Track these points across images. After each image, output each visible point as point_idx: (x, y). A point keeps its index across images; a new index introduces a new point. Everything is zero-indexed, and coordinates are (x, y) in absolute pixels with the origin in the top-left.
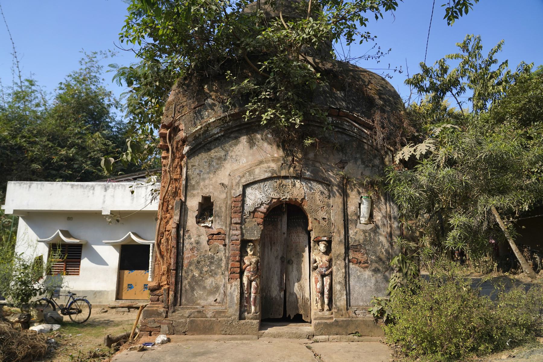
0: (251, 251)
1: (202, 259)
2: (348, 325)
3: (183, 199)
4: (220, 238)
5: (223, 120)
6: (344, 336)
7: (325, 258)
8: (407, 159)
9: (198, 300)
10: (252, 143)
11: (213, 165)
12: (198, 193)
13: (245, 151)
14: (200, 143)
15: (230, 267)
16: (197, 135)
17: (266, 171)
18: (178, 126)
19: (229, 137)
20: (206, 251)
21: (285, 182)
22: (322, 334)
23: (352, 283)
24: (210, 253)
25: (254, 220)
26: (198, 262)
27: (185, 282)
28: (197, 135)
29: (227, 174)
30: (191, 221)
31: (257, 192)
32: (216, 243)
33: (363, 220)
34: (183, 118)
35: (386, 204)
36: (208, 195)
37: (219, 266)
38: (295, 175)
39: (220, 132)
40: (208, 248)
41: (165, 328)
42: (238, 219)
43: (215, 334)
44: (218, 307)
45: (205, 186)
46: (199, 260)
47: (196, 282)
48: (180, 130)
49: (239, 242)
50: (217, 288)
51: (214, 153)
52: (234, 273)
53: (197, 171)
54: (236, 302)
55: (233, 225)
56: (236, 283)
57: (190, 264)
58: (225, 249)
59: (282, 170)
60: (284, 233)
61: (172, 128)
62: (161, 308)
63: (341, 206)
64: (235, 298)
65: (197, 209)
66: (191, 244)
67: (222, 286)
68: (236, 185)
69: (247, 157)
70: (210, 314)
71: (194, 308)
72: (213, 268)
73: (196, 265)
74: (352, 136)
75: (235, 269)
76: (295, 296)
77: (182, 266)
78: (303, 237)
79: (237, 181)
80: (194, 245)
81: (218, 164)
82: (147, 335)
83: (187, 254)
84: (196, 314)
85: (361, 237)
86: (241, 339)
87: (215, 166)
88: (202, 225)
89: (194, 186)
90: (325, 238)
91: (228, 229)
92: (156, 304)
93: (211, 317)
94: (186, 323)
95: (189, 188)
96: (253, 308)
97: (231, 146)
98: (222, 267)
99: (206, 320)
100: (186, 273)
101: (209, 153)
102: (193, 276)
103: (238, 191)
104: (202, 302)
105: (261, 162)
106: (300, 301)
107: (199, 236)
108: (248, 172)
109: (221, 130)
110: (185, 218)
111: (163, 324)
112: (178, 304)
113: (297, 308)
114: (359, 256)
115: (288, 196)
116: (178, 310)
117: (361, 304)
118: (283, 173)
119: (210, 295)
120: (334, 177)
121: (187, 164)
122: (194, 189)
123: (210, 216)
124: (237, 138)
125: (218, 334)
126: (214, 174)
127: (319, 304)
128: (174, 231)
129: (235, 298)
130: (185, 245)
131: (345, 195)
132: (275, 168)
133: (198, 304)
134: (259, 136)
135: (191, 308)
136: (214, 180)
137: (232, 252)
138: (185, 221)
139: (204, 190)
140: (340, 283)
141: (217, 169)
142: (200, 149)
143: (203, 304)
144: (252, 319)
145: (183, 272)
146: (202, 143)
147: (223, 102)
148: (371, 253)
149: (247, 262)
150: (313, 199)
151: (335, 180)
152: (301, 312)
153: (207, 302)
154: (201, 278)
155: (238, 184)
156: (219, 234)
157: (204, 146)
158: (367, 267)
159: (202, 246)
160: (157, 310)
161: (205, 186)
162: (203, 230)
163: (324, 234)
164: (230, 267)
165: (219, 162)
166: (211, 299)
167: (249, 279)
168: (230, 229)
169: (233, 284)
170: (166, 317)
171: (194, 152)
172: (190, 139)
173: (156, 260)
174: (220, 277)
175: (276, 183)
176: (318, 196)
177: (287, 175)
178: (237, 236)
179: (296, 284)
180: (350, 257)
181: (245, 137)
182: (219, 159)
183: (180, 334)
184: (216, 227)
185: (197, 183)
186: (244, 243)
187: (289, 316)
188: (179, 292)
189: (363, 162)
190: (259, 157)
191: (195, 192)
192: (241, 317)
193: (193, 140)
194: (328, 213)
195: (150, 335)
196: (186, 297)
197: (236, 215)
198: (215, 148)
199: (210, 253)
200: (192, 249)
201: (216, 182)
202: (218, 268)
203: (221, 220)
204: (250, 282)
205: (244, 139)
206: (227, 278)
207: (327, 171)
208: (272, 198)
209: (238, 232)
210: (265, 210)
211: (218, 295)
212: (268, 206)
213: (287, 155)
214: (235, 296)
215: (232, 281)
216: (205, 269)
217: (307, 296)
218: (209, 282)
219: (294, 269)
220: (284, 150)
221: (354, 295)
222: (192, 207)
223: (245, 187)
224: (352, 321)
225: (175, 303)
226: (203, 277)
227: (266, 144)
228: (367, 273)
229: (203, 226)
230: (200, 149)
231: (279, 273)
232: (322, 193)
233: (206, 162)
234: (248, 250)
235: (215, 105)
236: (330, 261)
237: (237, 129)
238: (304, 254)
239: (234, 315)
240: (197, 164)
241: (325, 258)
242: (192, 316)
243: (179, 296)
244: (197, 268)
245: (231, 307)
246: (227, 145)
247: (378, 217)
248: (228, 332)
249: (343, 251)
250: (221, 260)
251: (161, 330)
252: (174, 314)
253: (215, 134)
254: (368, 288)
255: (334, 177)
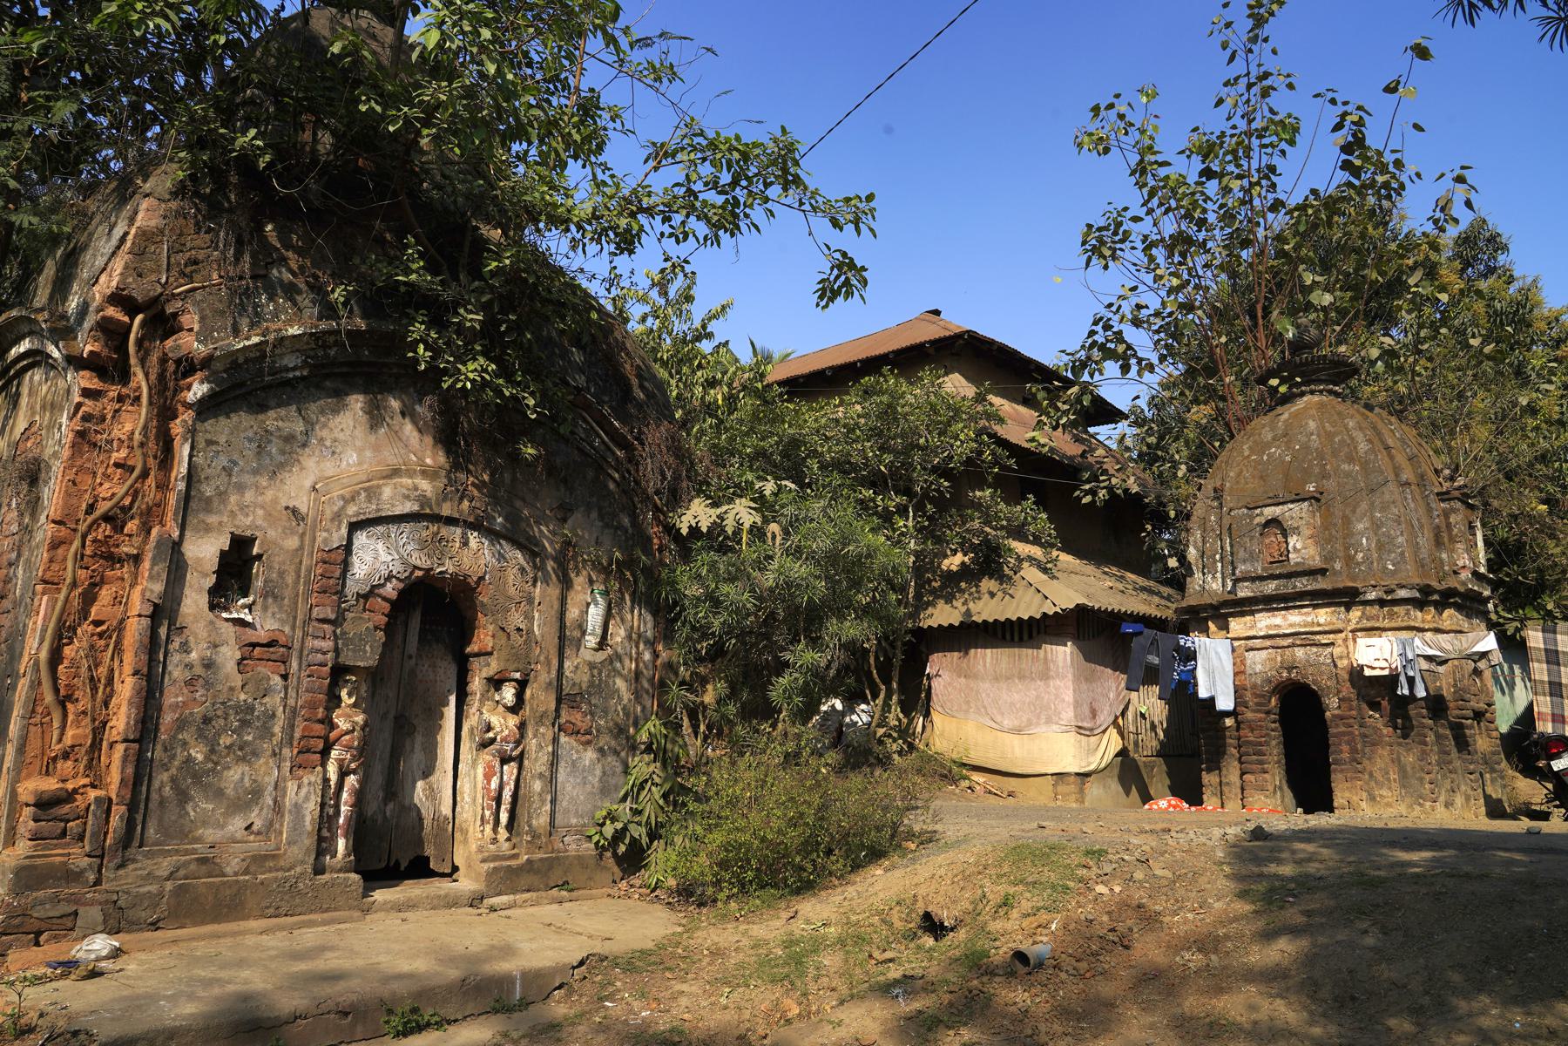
0: (350, 695)
1: (219, 713)
2: (550, 868)
3: (176, 534)
4: (273, 657)
5: (318, 339)
6: (543, 894)
7: (513, 721)
8: (704, 530)
9: (197, 828)
10: (376, 417)
11: (269, 454)
12: (220, 523)
13: (357, 432)
14: (242, 385)
15: (297, 735)
16: (241, 360)
17: (407, 497)
18: (175, 315)
19: (318, 387)
20: (232, 689)
21: (445, 531)
22: (499, 894)
23: (561, 775)
24: (242, 697)
25: (366, 615)
26: (207, 720)
27: (162, 778)
28: (241, 360)
29: (308, 483)
30: (194, 601)
31: (380, 546)
32: (263, 669)
33: (591, 641)
34: (198, 295)
35: (632, 612)
36: (248, 533)
37: (266, 732)
38: (471, 519)
39: (302, 368)
40: (237, 680)
41: (93, 914)
42: (329, 609)
43: (246, 918)
44: (255, 845)
45: (243, 508)
46: (210, 714)
47: (197, 778)
48: (181, 329)
49: (327, 669)
50: (256, 793)
51: (273, 419)
52: (308, 751)
53: (223, 461)
54: (309, 827)
55: (315, 624)
56: (313, 779)
57: (181, 724)
58: (286, 688)
59: (444, 500)
60: (410, 657)
61: (152, 312)
62: (78, 857)
63: (556, 605)
64: (308, 819)
65: (215, 568)
66: (189, 666)
67: (270, 788)
68: (332, 520)
69: (360, 451)
70: (233, 865)
71: (187, 852)
72: (250, 738)
73: (199, 729)
74: (587, 455)
75: (312, 742)
76: (414, 814)
77: (157, 729)
78: (446, 673)
79: (336, 509)
80: (198, 670)
81: (283, 452)
82: (26, 946)
83: (172, 697)
84: (193, 867)
85: (584, 678)
86: (324, 923)
87: (281, 455)
88: (225, 615)
89: (209, 500)
90: (518, 675)
91: (299, 633)
92: (56, 847)
93: (236, 874)
94: (161, 895)
95: (193, 505)
96: (341, 844)
97: (322, 412)
98: (273, 735)
99: (224, 883)
100: (166, 750)
101: (261, 417)
102: (189, 760)
103: (335, 535)
104: (210, 834)
105: (395, 472)
106: (427, 822)
107: (216, 646)
108: (365, 490)
109: (305, 362)
110: (177, 591)
111: (85, 904)
112: (136, 843)
113: (420, 842)
114: (576, 717)
115: (449, 567)
116: (134, 861)
117: (574, 821)
118: (446, 510)
119: (234, 813)
120: (547, 536)
121: (192, 432)
122: (208, 510)
123: (246, 596)
124: (340, 394)
125: (256, 918)
126: (271, 478)
127: (488, 828)
128: (135, 629)
129: (308, 819)
130: (170, 668)
131: (566, 584)
132: (429, 494)
133: (198, 840)
134: (395, 404)
135: (177, 852)
136: (270, 494)
137: (306, 697)
138: (178, 601)
139: (240, 517)
140: (541, 776)
141: (282, 466)
142: (236, 398)
143: (210, 839)
144: (340, 871)
145: (159, 747)
146: (246, 386)
147: (318, 289)
148: (599, 712)
149: (343, 724)
150: (501, 580)
151: (551, 543)
152: (429, 851)
153: (225, 832)
154: (210, 765)
155: (337, 516)
156: (271, 644)
157: (250, 393)
158: (589, 743)
159: (221, 676)
160: (65, 864)
161: (243, 508)
162: (229, 631)
163: (515, 665)
164: (297, 735)
165: (288, 448)
166: (237, 825)
167: (341, 767)
168: (305, 634)
169: (305, 780)
170: (98, 882)
171: (219, 404)
172: (218, 366)
173: (33, 711)
174: (267, 763)
175: (426, 531)
176: (512, 574)
177: (456, 515)
178: (324, 653)
179: (420, 784)
180: (563, 720)
181: (361, 398)
182: (289, 439)
183: (141, 930)
184: (266, 624)
185: (220, 494)
186: (339, 673)
187: (397, 863)
188: (142, 806)
189: (601, 517)
190: (391, 456)
191: (212, 519)
192: (319, 870)
193: (225, 371)
194: (529, 617)
195: (37, 944)
196: (160, 820)
197: (325, 598)
198: (279, 406)
199: (242, 697)
200: (189, 683)
201: (275, 501)
202: (262, 738)
203: (281, 607)
204: (343, 774)
205: (357, 402)
206: (288, 764)
207: (538, 523)
208: (416, 567)
209: (327, 645)
210: (394, 595)
211: (256, 811)
212: (401, 586)
213: (456, 466)
214: (307, 813)
215: (300, 772)
216: (225, 740)
217: (446, 810)
218: (235, 775)
219: (418, 747)
220: (448, 453)
221: (563, 803)
222: (198, 560)
223: (354, 527)
224: (557, 858)
225: (126, 840)
226: (216, 764)
227: (408, 428)
228: (590, 755)
229: (227, 620)
230: (236, 398)
231: (387, 755)
232: (522, 570)
233: (250, 440)
234: (344, 694)
235: (300, 292)
236: (522, 727)
237: (345, 370)
238: (445, 710)
239: (303, 862)
240: (222, 440)
241: (513, 721)
242: (182, 872)
243: (139, 818)
244: (200, 736)
245: (295, 843)
246: (313, 407)
247: (618, 634)
248: (282, 911)
249: (553, 706)
250: (274, 715)
251: (79, 923)
252: (121, 872)
253: (288, 370)
254: (589, 787)
255: (547, 536)
